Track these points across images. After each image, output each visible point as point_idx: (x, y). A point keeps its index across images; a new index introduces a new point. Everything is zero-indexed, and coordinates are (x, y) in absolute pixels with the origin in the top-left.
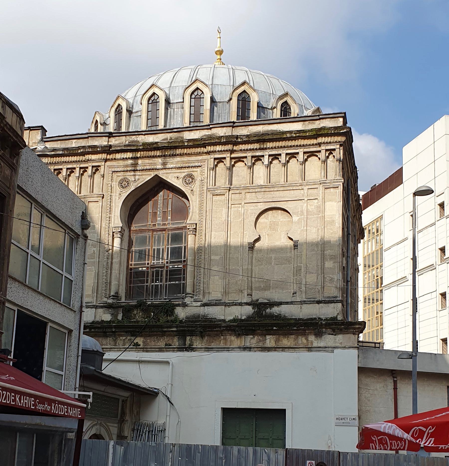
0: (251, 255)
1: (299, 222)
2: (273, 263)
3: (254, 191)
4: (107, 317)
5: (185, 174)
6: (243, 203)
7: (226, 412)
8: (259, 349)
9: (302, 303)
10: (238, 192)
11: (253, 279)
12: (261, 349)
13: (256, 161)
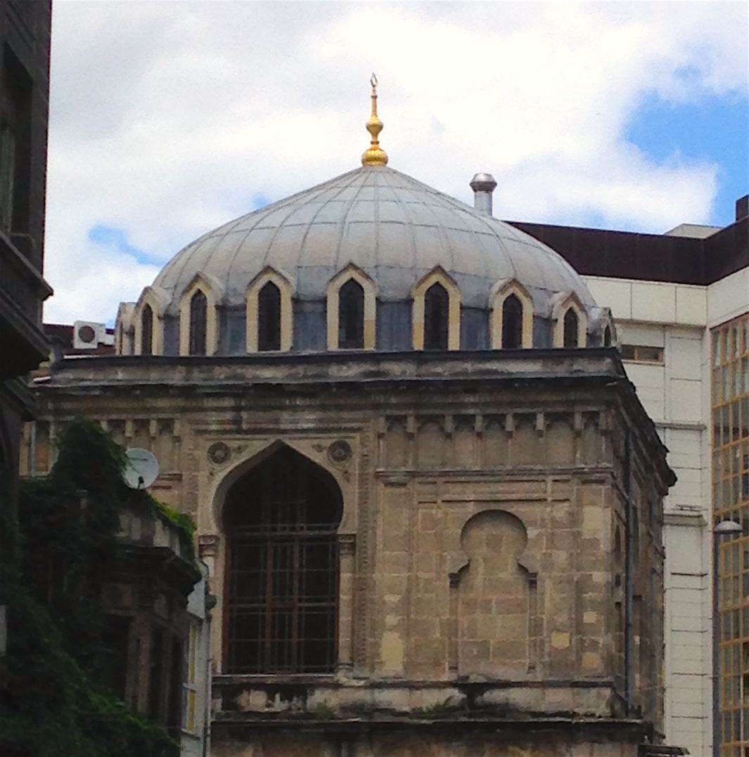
5: (334, 440)
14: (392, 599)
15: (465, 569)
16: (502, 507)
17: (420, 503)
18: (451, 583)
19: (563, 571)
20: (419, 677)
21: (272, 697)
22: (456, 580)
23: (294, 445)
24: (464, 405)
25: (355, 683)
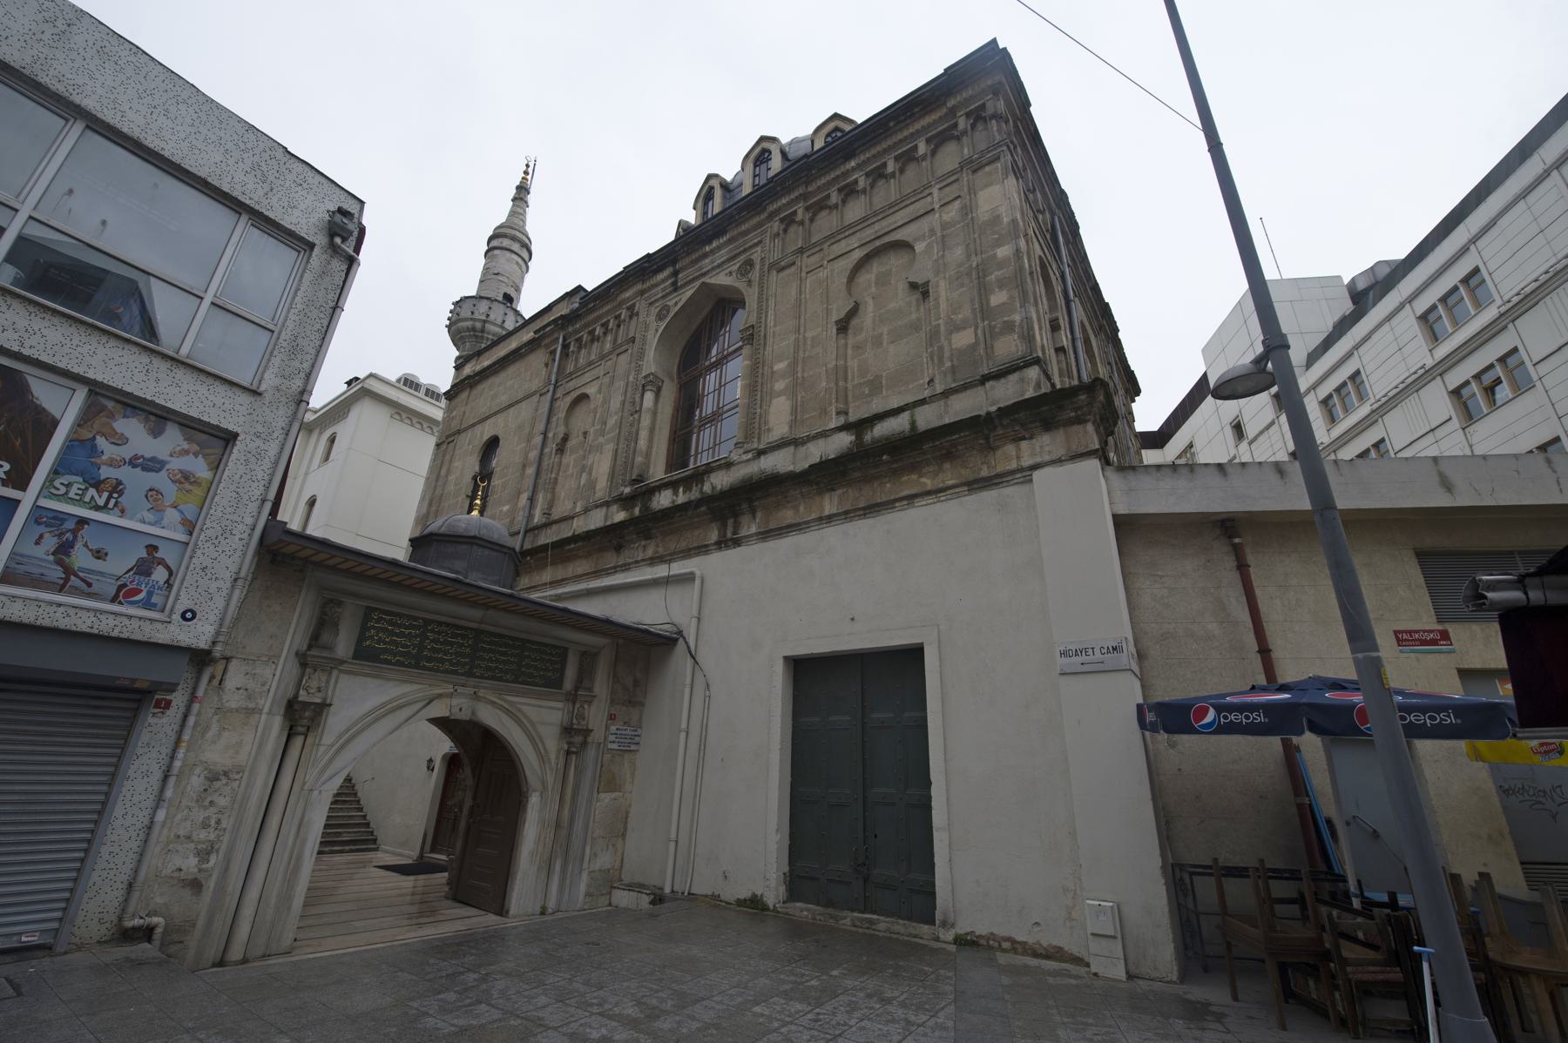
1: (929, 247)
4: (620, 516)
7: (803, 670)
9: (946, 394)
11: (850, 386)
13: (847, 195)
14: (780, 366)
15: (854, 312)
16: (887, 239)
19: (959, 266)
20: (802, 433)
21: (676, 493)
22: (843, 326)
23: (712, 281)
24: (846, 174)
25: (745, 457)
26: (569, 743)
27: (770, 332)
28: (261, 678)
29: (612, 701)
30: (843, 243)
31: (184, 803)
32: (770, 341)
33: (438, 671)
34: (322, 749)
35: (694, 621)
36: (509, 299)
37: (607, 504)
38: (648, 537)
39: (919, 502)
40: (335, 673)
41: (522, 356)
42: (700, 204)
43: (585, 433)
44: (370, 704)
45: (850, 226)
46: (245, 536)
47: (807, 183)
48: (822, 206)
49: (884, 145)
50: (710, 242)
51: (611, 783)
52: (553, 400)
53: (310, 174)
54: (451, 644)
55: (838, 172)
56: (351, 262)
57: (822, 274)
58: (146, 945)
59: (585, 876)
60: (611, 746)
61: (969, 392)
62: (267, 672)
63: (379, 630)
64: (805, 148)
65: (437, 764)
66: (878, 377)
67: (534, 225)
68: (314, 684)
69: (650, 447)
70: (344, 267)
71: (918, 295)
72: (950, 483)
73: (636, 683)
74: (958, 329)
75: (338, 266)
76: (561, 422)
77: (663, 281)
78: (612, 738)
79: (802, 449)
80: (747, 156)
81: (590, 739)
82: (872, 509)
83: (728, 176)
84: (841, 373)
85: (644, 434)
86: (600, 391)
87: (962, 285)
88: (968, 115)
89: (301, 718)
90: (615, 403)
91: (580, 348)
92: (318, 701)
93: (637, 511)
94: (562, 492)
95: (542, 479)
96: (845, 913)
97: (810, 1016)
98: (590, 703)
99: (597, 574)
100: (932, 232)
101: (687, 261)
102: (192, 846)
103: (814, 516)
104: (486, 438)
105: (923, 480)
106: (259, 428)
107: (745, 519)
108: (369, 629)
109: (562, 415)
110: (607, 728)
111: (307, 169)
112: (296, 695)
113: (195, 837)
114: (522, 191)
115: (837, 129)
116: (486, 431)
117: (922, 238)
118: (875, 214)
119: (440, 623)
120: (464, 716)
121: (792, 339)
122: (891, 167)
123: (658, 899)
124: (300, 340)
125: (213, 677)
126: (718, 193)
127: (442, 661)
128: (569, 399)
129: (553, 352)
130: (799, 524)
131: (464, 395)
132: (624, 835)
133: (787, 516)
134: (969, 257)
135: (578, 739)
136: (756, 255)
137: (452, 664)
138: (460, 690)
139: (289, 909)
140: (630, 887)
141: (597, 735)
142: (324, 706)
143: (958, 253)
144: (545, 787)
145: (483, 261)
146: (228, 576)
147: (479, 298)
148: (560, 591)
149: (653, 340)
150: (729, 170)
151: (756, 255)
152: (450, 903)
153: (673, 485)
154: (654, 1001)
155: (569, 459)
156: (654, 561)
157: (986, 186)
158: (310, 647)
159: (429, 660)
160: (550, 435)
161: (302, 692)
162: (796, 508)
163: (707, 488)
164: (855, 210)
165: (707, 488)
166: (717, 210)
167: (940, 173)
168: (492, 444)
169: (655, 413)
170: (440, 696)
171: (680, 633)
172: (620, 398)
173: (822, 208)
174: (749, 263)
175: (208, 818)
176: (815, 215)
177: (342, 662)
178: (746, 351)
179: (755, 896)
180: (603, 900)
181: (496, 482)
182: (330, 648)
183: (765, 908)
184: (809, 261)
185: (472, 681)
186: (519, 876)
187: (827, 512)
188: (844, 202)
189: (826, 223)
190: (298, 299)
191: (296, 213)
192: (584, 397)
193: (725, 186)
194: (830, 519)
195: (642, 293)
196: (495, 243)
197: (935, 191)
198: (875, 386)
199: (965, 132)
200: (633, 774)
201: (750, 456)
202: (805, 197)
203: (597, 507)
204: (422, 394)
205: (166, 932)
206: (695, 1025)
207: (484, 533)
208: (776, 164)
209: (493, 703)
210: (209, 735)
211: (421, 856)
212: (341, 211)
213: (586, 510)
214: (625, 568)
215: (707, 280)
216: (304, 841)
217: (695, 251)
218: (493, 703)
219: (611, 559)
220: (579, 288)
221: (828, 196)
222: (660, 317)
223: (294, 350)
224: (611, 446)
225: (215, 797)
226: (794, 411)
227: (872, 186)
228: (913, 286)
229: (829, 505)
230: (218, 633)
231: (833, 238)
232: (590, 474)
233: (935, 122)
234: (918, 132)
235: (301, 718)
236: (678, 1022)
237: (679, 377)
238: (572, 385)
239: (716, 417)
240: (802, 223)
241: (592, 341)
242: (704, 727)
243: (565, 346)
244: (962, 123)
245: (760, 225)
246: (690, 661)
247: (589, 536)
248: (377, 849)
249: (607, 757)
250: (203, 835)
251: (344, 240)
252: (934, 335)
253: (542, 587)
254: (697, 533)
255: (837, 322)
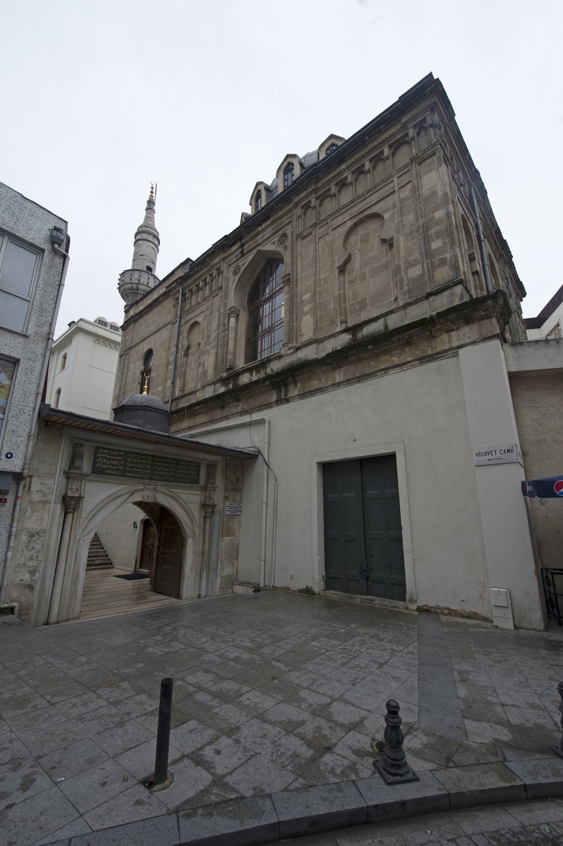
0: (342, 279)
1: (393, 216)
2: (367, 278)
3: (339, 213)
4: (222, 390)
5: (278, 237)
6: (330, 231)
7: (328, 469)
8: (355, 380)
10: (324, 223)
11: (347, 305)
12: (357, 380)
13: (341, 187)
14: (306, 297)
15: (348, 260)
16: (366, 213)
17: (320, 238)
18: (339, 272)
19: (412, 225)
20: (321, 335)
22: (342, 270)
23: (264, 248)
25: (289, 352)
26: (205, 512)
27: (299, 277)
28: (48, 486)
29: (226, 490)
30: (340, 218)
31: (19, 549)
32: (299, 282)
33: (135, 477)
34: (82, 520)
35: (266, 445)
36: (149, 269)
37: (214, 383)
38: (238, 400)
39: (391, 372)
40: (84, 481)
41: (160, 302)
42: (253, 202)
43: (199, 344)
44: (103, 496)
45: (344, 207)
46: (31, 413)
47: (316, 183)
48: (326, 196)
49: (363, 152)
50: (260, 225)
51: (229, 532)
52: (180, 326)
53: (37, 208)
54: (140, 463)
55: (335, 173)
56: (65, 258)
57: (328, 238)
58: (11, 616)
59: (219, 579)
60: (227, 513)
61: (419, 304)
62: (51, 482)
63: (103, 458)
64: (314, 160)
65: (139, 524)
66: (364, 299)
67: (159, 224)
68: (74, 487)
69: (235, 349)
70: (62, 261)
71: (387, 247)
72: (409, 359)
73: (237, 480)
74: (412, 265)
75: (58, 261)
76: (185, 338)
77: (235, 251)
78: (227, 509)
79: (321, 345)
80: (279, 168)
81: (216, 510)
82: (364, 377)
83: (269, 182)
84: (342, 298)
85: (231, 342)
86: (205, 319)
87: (414, 238)
88: (415, 127)
89: (70, 505)
90: (214, 326)
91: (192, 295)
92: (77, 495)
93: (231, 386)
94: (189, 378)
95: (178, 372)
96: (356, 596)
97: (341, 647)
98: (214, 491)
99: (212, 422)
100: (394, 205)
101: (248, 237)
102: (26, 569)
103: (330, 383)
104: (145, 350)
105: (393, 358)
106: (30, 355)
107: (291, 387)
108: (98, 458)
109: (185, 334)
110: (224, 504)
111: (35, 206)
112: (66, 493)
113: (27, 565)
114: (151, 203)
115: (333, 145)
116: (145, 347)
117: (388, 210)
118: (359, 197)
119: (133, 453)
120: (150, 500)
121: (313, 279)
122: (367, 166)
123: (257, 590)
124: (44, 305)
125: (25, 486)
126: (264, 194)
127: (137, 473)
128: (188, 325)
129: (177, 299)
130: (322, 388)
131: (131, 327)
132: (237, 558)
133: (315, 384)
134: (417, 220)
135: (210, 510)
136: (288, 230)
137: (142, 474)
138: (147, 487)
139: (76, 597)
140: (242, 584)
141: (219, 507)
142: (80, 499)
143: (410, 218)
144: (195, 535)
145: (133, 248)
146: (25, 434)
147: (133, 270)
148: (193, 432)
149: (232, 287)
150: (269, 177)
151: (288, 230)
152: (152, 593)
153: (249, 370)
154: (260, 640)
155: (191, 359)
156: (243, 413)
157: (428, 172)
158: (70, 469)
159: (130, 472)
160: (180, 346)
161: (69, 492)
162: (320, 379)
163: (269, 371)
164: (346, 196)
165: (269, 371)
166: (264, 204)
167: (398, 167)
168: (149, 354)
169: (236, 330)
170: (137, 490)
171: (259, 452)
172: (217, 323)
173: (326, 197)
174: (285, 236)
175: (32, 555)
176: (322, 201)
177: (87, 475)
178: (286, 289)
179: (308, 587)
180: (229, 591)
181: (153, 374)
182: (79, 468)
183: (313, 594)
184: (320, 231)
185: (153, 482)
186: (186, 579)
187: (337, 381)
188: (339, 191)
189: (329, 206)
190: (40, 282)
191: (33, 232)
192: (196, 324)
193: (268, 189)
194: (339, 384)
195: (224, 259)
196: (139, 237)
197: (395, 179)
198: (363, 305)
199: (413, 139)
200: (239, 527)
201: (292, 351)
202: (315, 191)
203: (209, 385)
204: (108, 328)
205: (20, 609)
206: (282, 651)
207: (151, 404)
208: (297, 171)
209: (164, 493)
210: (27, 515)
211: (135, 570)
212: (56, 229)
213: (203, 387)
214: (227, 418)
215: (260, 248)
216: (79, 565)
217: (252, 231)
218: (164, 493)
219: (219, 413)
220: (188, 260)
221: (330, 189)
222: (235, 273)
223: (42, 311)
224: (214, 351)
225: (34, 545)
226: (316, 323)
227: (356, 180)
228: (384, 241)
229: (339, 376)
230: (24, 464)
231: (333, 215)
232: (203, 367)
233: (394, 134)
234: (383, 141)
235: (70, 505)
236: (273, 650)
237: (249, 308)
238: (189, 317)
239: (271, 330)
240: (314, 208)
241: (198, 290)
242: (276, 502)
243: (184, 295)
244: (411, 132)
245: (290, 211)
246: (265, 467)
247: (206, 401)
248: (113, 568)
249: (225, 518)
250: (31, 563)
251: (60, 245)
252: (397, 271)
253: (184, 431)
254: (264, 397)
255: (338, 268)
